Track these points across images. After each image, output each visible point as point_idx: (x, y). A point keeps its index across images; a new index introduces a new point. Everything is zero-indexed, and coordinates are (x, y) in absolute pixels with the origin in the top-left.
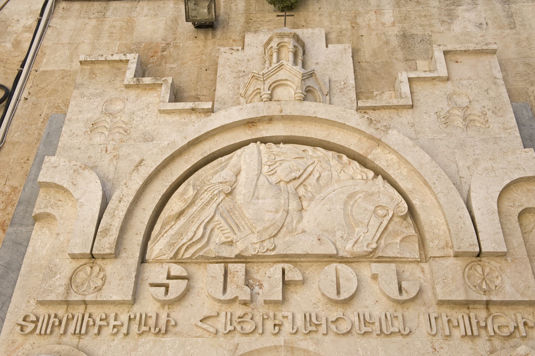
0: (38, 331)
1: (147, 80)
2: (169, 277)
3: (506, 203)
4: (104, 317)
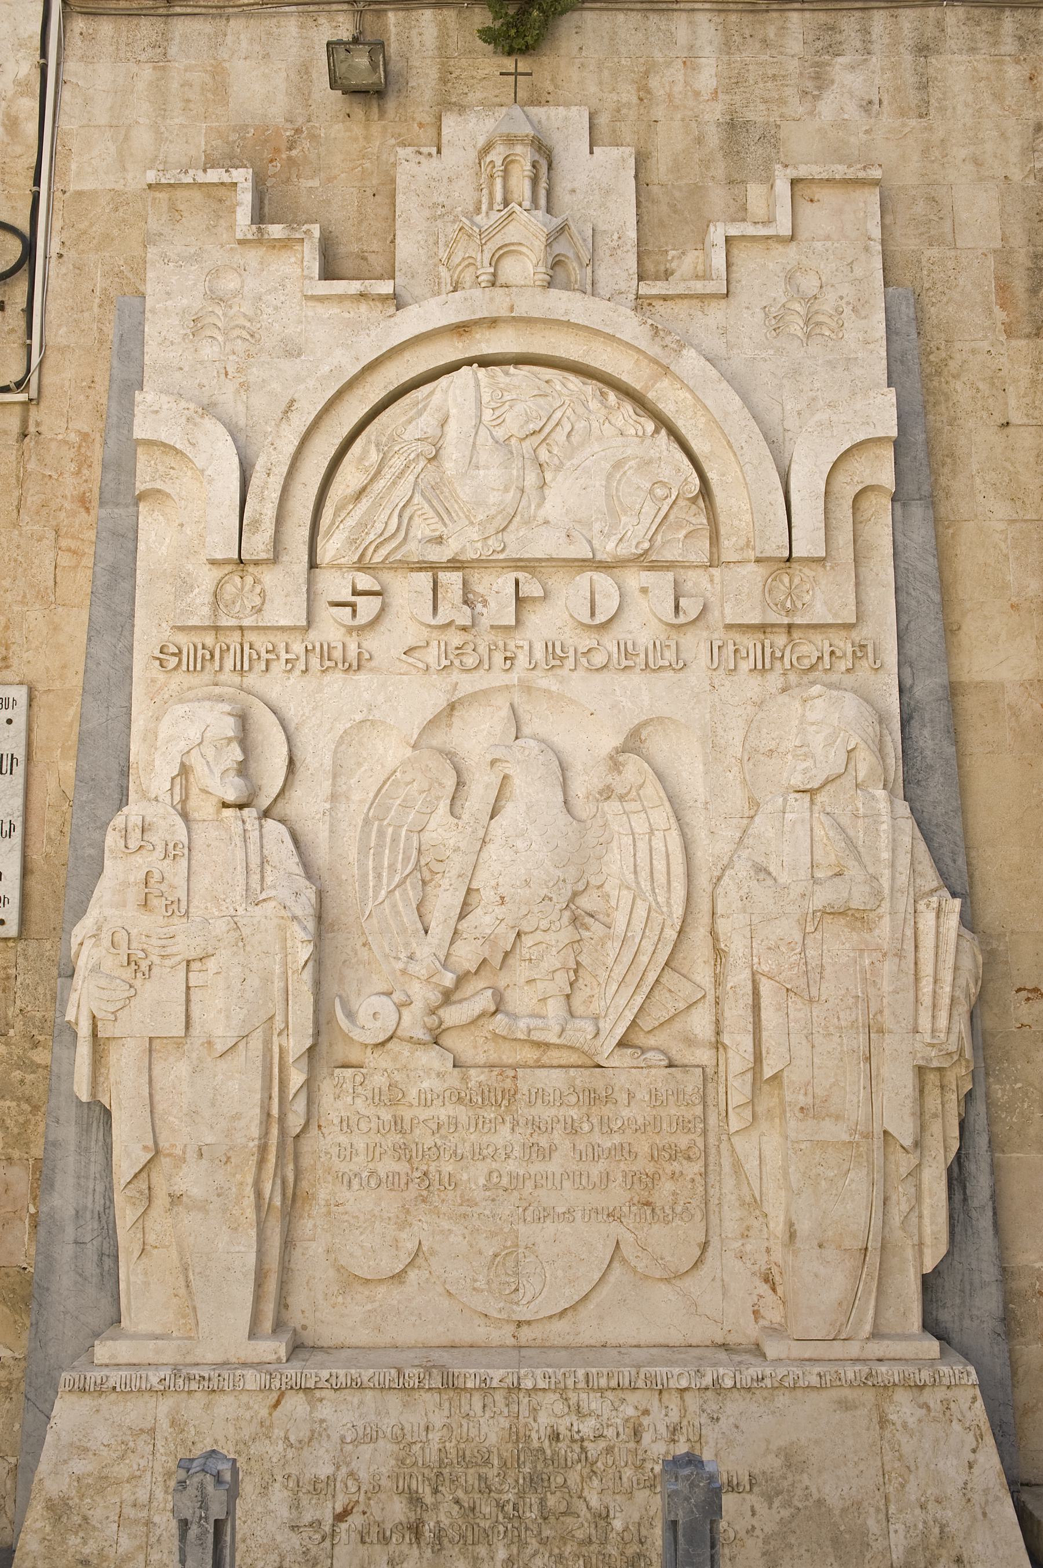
0: (184, 668)
1: (276, 231)
2: (355, 593)
3: (841, 478)
4: (270, 648)
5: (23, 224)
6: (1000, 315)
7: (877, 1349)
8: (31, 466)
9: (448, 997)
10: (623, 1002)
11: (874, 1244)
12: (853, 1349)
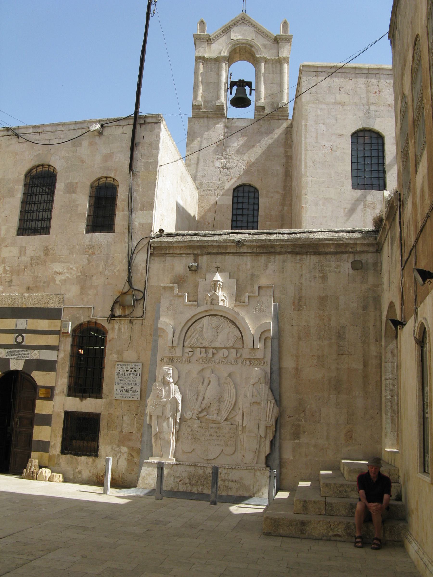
3: (263, 335)
5: (143, 290)
6: (293, 307)
7: (256, 465)
8: (143, 329)
9: (200, 412)
10: (225, 414)
11: (257, 451)
12: (253, 465)
